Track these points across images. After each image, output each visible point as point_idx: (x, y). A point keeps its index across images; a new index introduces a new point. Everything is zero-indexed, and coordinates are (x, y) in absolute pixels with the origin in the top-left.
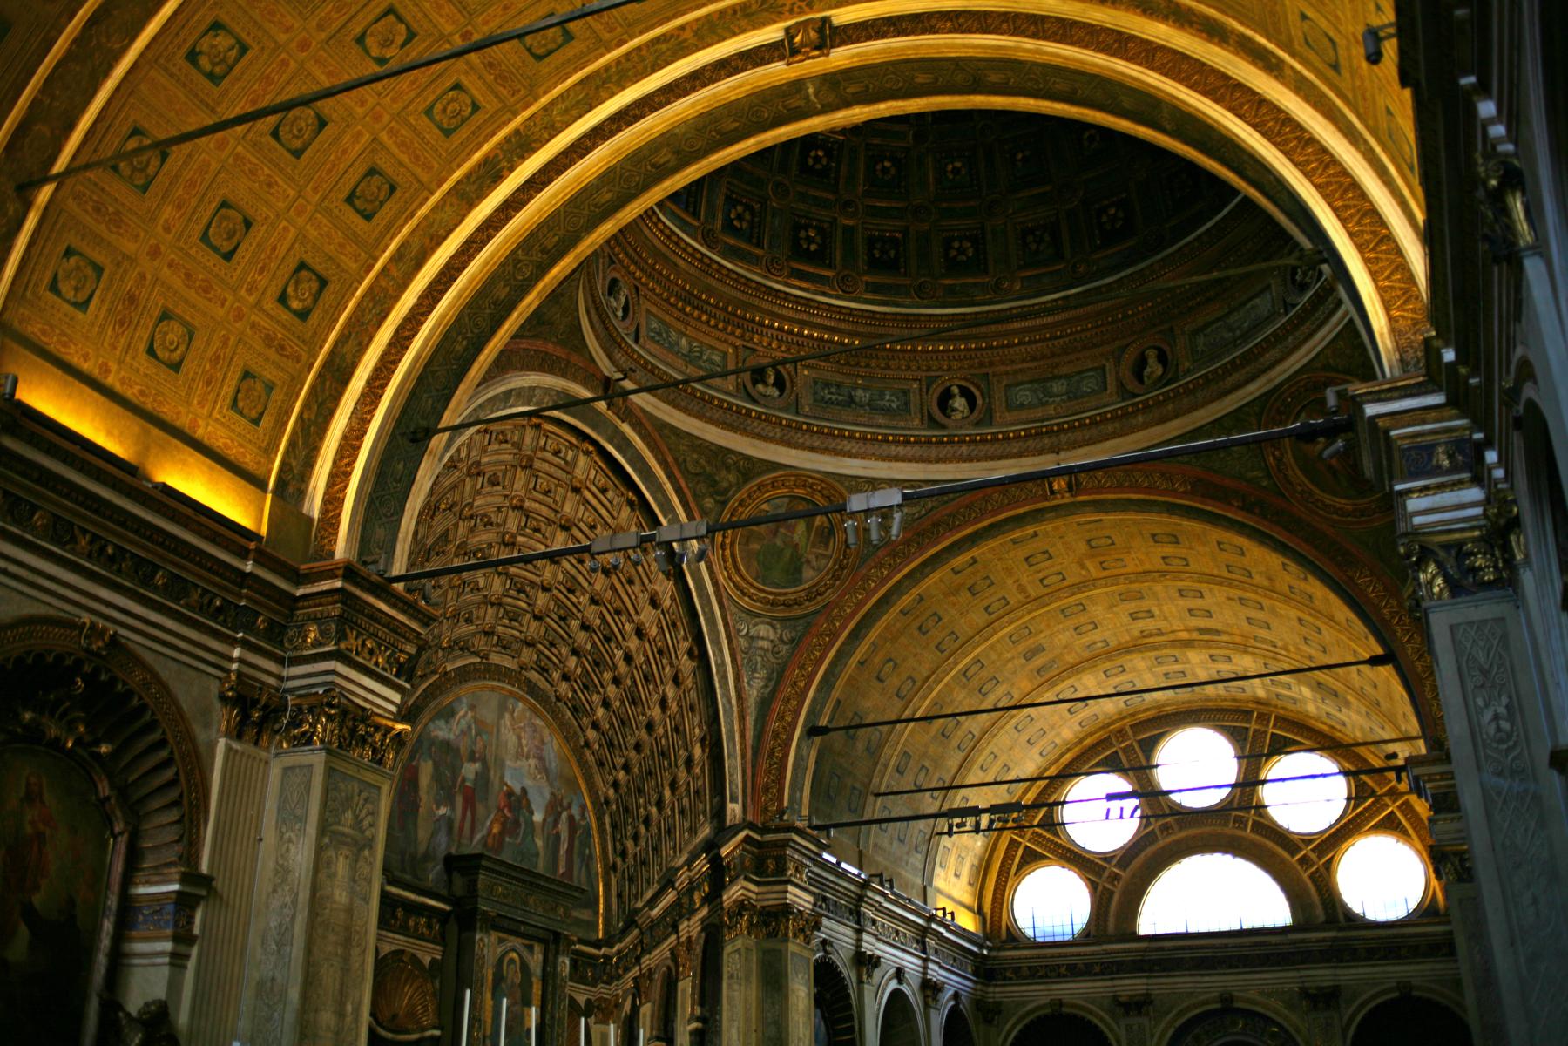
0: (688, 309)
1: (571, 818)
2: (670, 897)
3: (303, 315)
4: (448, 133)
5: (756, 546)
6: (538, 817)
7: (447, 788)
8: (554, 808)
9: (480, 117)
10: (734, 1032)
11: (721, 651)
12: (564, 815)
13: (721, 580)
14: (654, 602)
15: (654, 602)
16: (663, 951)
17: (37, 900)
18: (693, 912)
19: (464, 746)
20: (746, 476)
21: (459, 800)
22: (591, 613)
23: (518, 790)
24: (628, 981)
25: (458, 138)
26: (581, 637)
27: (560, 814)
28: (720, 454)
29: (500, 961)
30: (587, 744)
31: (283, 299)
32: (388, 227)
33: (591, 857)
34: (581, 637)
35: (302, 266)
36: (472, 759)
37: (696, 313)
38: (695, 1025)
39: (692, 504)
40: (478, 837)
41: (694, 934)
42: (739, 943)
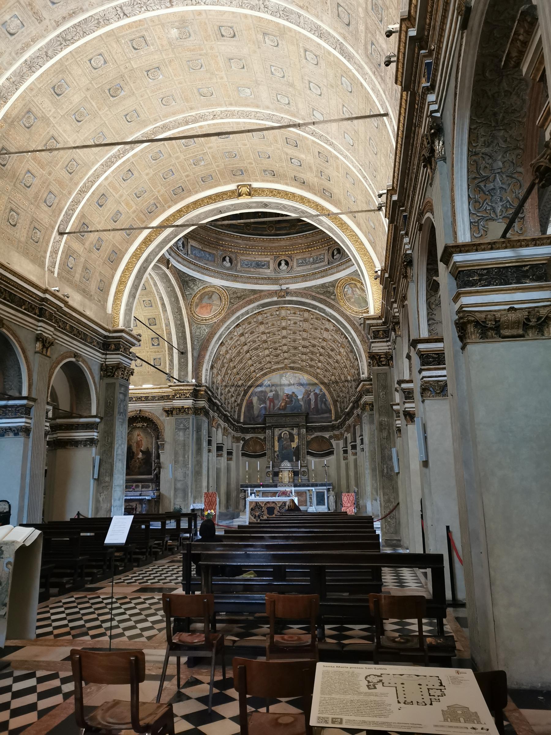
0: (310, 249)
1: (316, 394)
2: (351, 404)
3: (158, 345)
4: (152, 306)
5: (353, 300)
6: (300, 397)
7: (262, 400)
8: (307, 394)
9: (152, 301)
10: (366, 439)
11: (351, 334)
12: (312, 394)
13: (348, 313)
14: (327, 330)
15: (327, 330)
16: (351, 420)
17: (142, 449)
18: (357, 408)
19: (268, 389)
20: (334, 286)
21: (268, 402)
22: (306, 343)
23: (290, 393)
24: (344, 428)
25: (153, 305)
26: (305, 350)
27: (310, 394)
28: (323, 286)
29: (281, 434)
30: (318, 373)
31: (153, 345)
32: (160, 323)
33: (326, 400)
34: (305, 350)
35: (152, 339)
36: (271, 391)
37: (313, 249)
38: (361, 437)
39: (328, 300)
40: (276, 408)
41: (360, 413)
42: (366, 414)
